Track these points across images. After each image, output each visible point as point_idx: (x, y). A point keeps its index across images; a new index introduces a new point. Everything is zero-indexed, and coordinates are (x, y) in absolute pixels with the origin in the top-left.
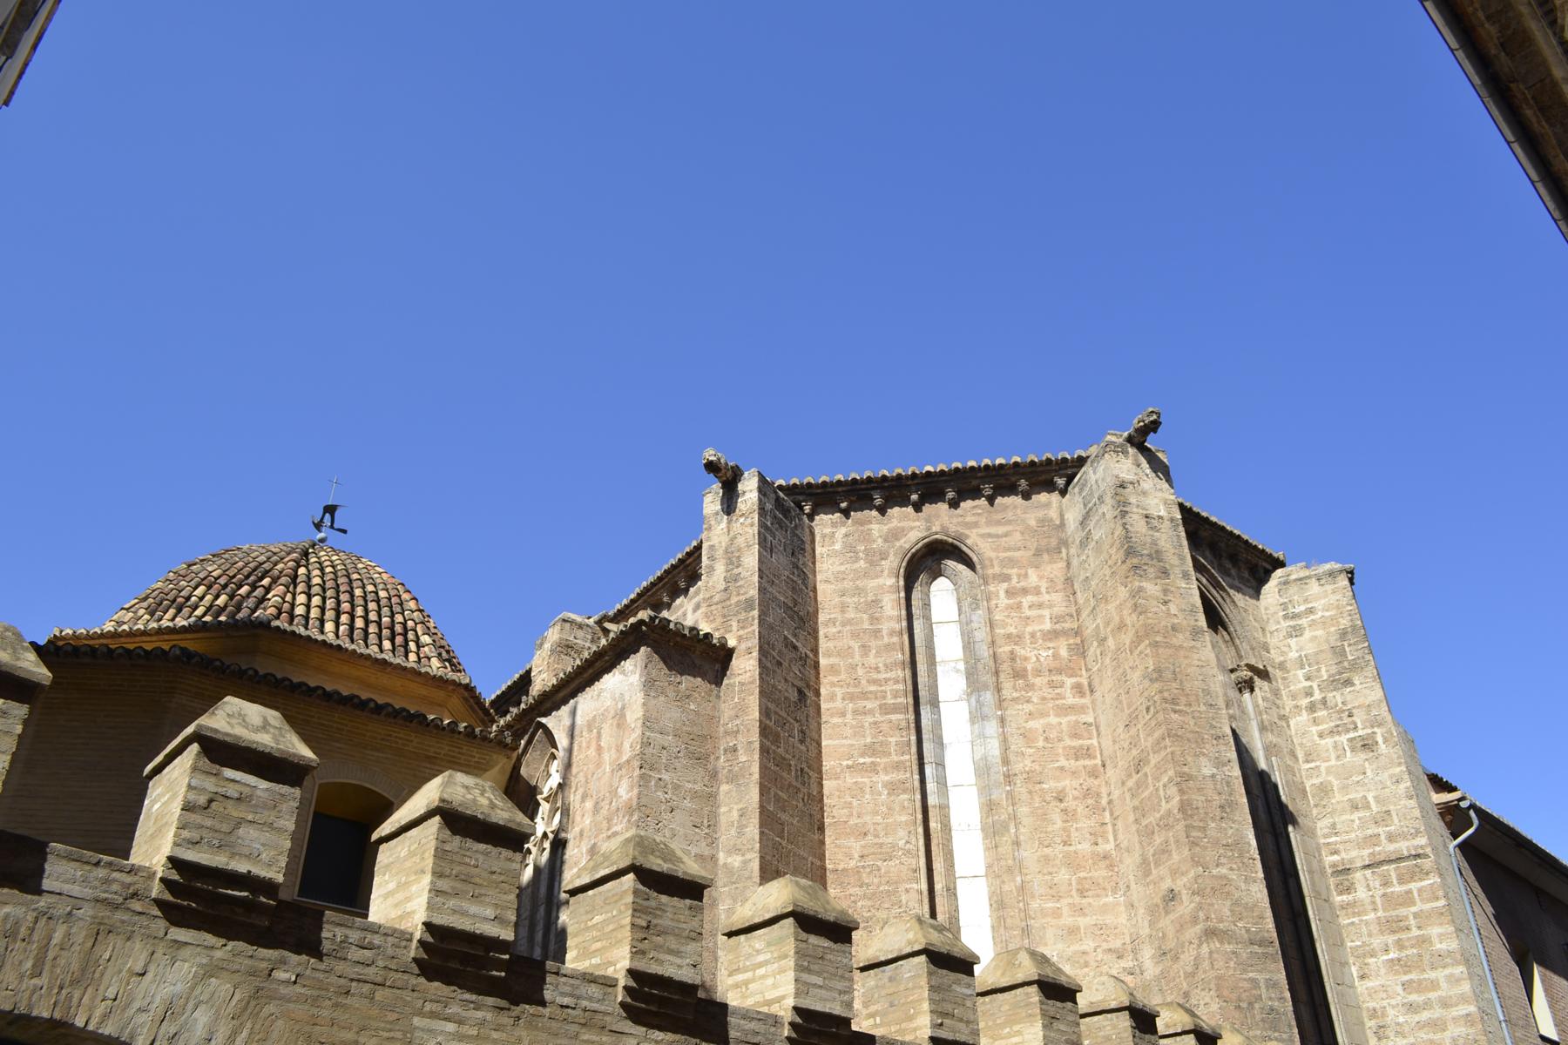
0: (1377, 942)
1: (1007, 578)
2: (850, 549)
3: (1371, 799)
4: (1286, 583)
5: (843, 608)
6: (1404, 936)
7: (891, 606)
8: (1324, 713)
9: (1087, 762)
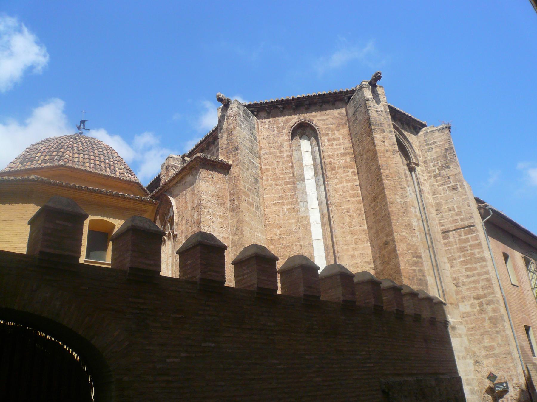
0: (456, 255)
1: (327, 135)
3: (455, 207)
4: (427, 133)
5: (270, 148)
6: (466, 253)
8: (440, 178)
9: (357, 199)
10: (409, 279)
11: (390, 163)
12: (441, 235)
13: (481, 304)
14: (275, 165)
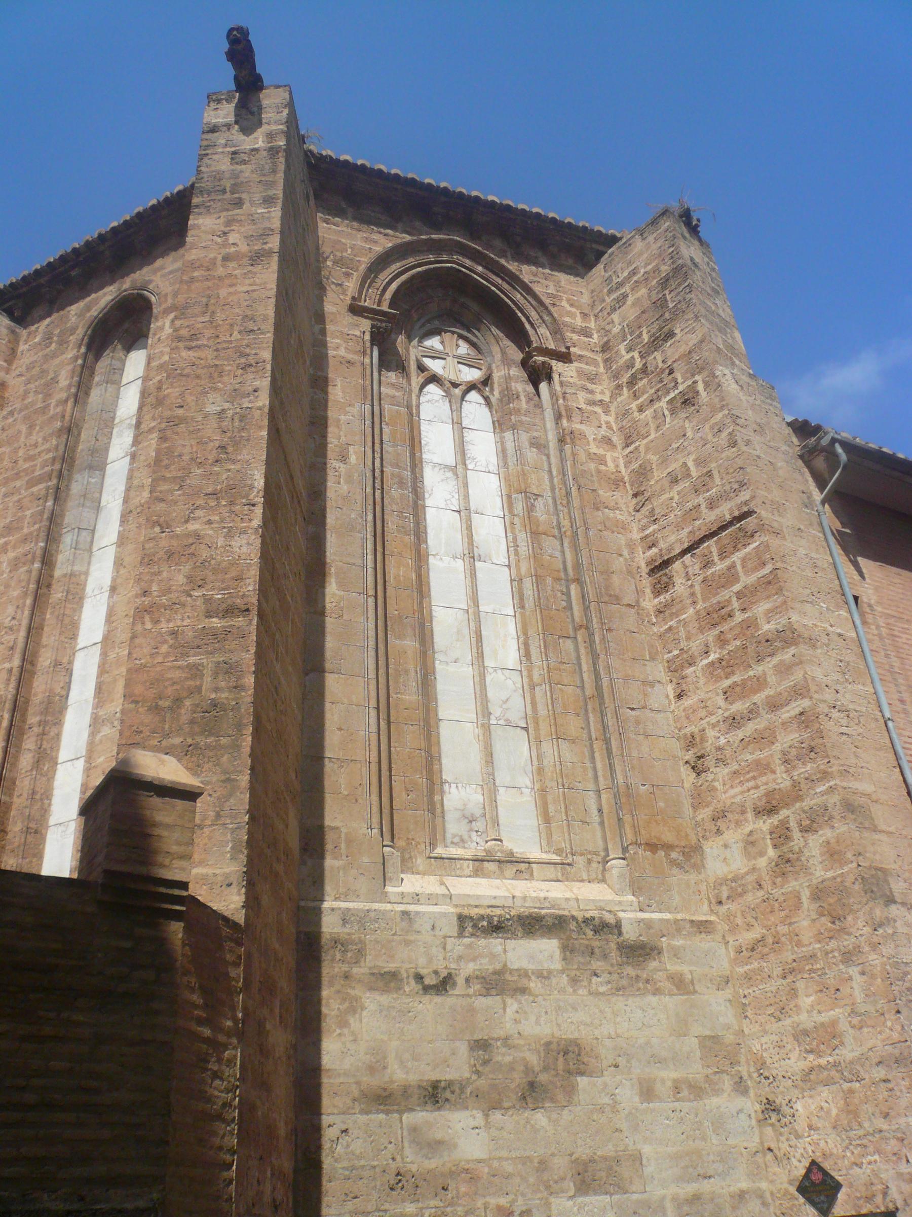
0: (695, 646)
2: (48, 337)
3: (690, 464)
6: (725, 627)
7: (65, 379)
8: (645, 381)
10: (155, 709)
11: (223, 292)
12: (646, 583)
13: (781, 835)
14: (22, 439)
